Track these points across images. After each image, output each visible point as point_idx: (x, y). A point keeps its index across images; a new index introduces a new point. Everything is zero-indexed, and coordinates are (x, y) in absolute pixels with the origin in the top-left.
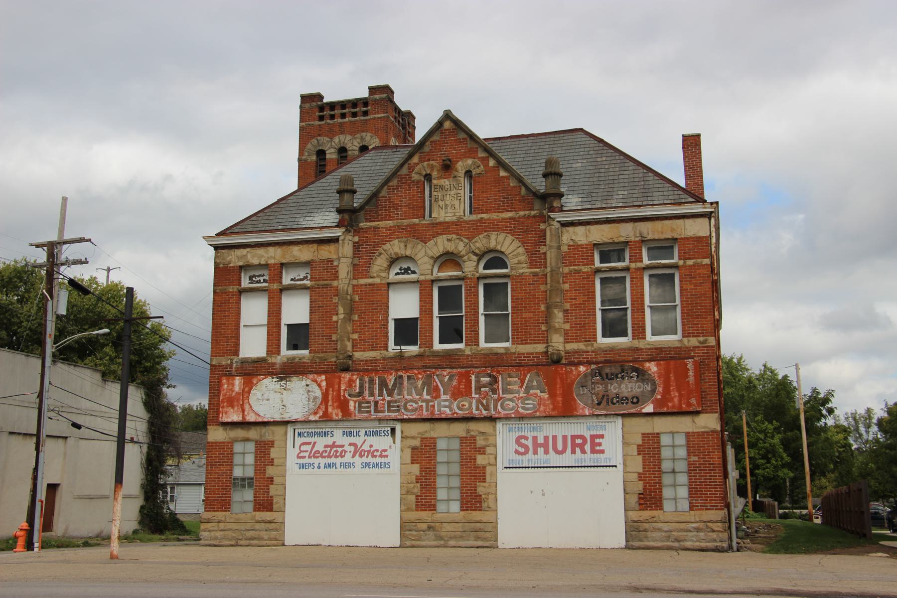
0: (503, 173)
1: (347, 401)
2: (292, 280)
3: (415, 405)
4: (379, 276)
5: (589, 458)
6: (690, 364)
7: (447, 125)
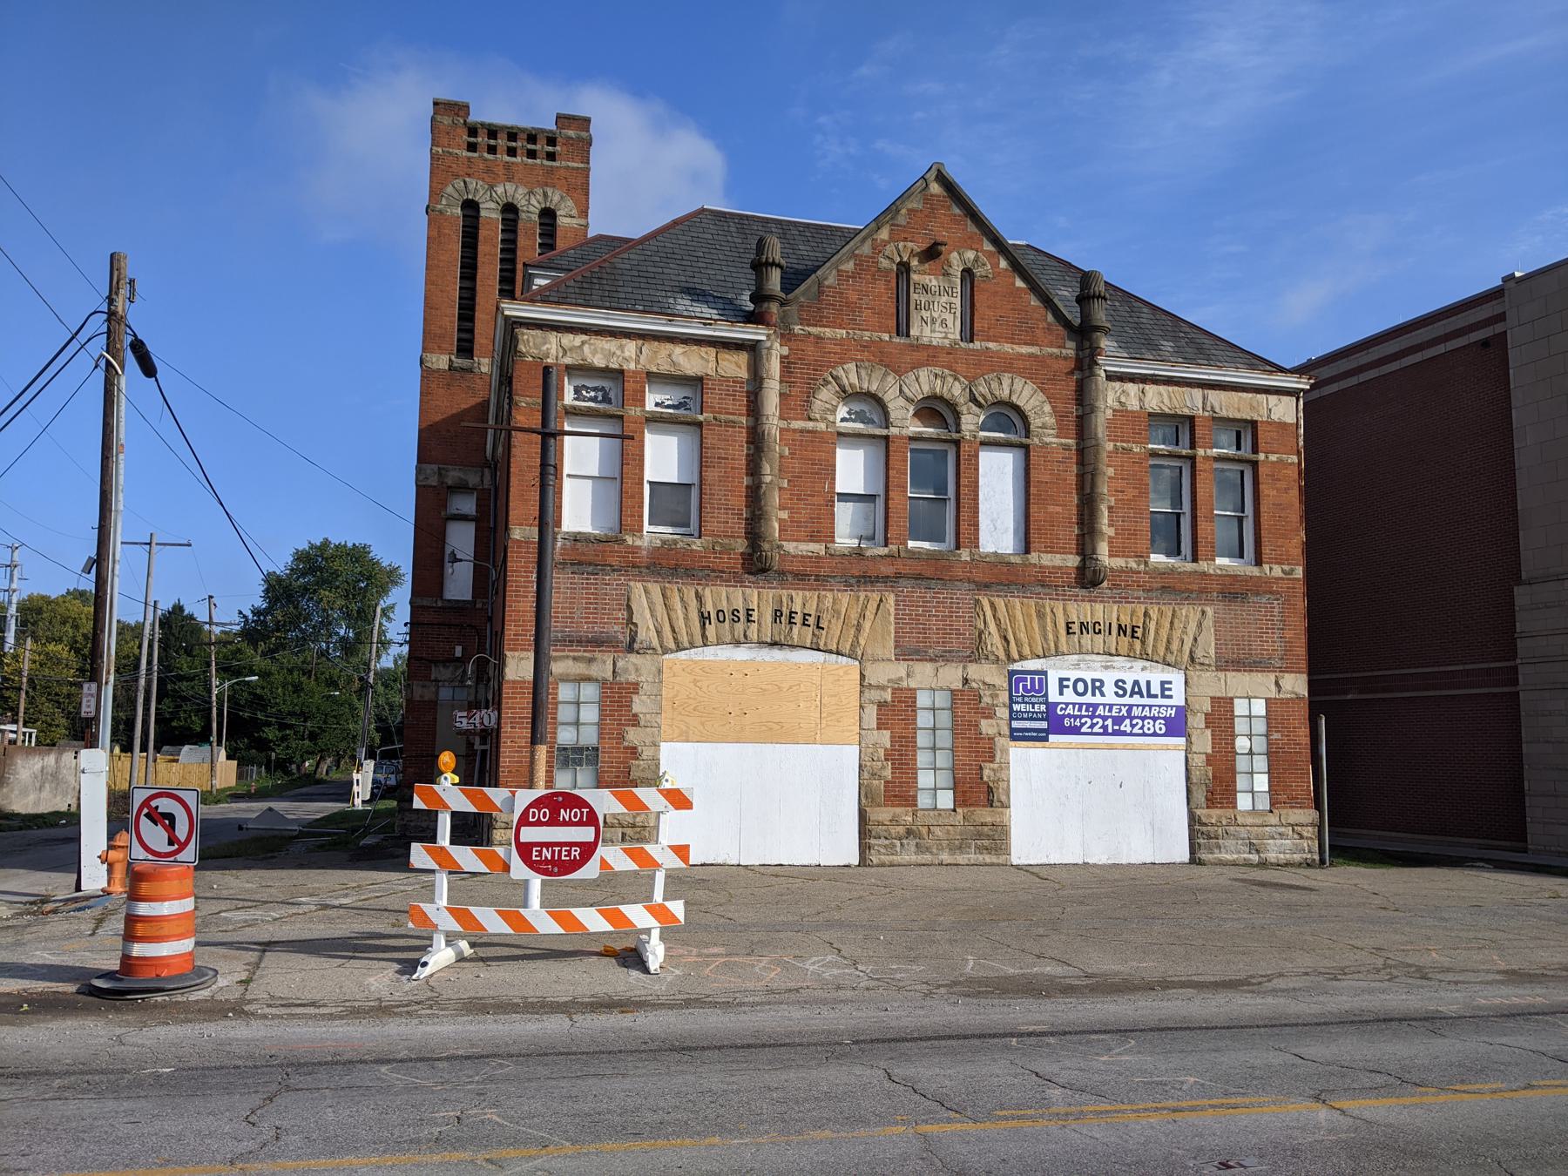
0: (1019, 283)
2: (657, 404)
4: (824, 419)
7: (935, 188)
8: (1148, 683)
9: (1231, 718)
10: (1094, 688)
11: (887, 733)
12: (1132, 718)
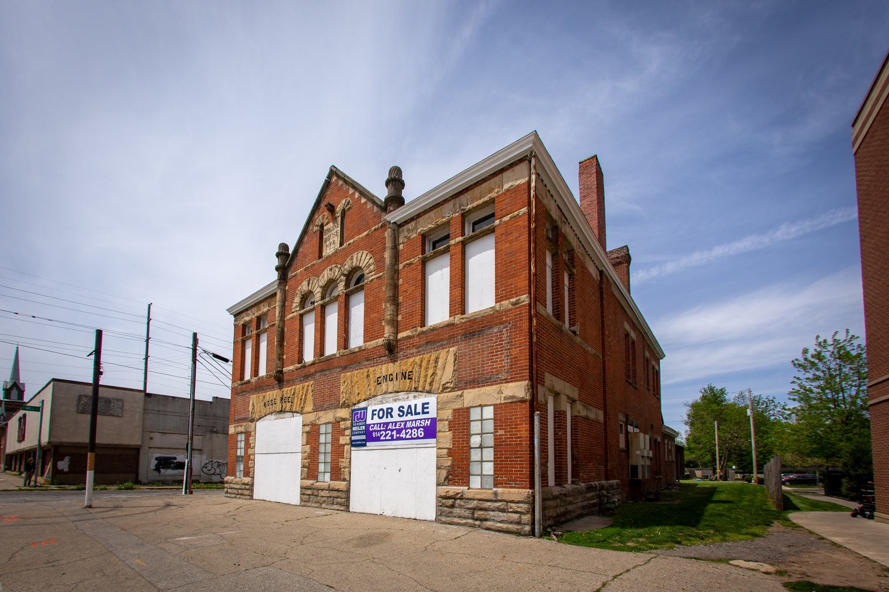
8: (416, 405)
9: (468, 423)
10: (388, 413)
12: (406, 429)
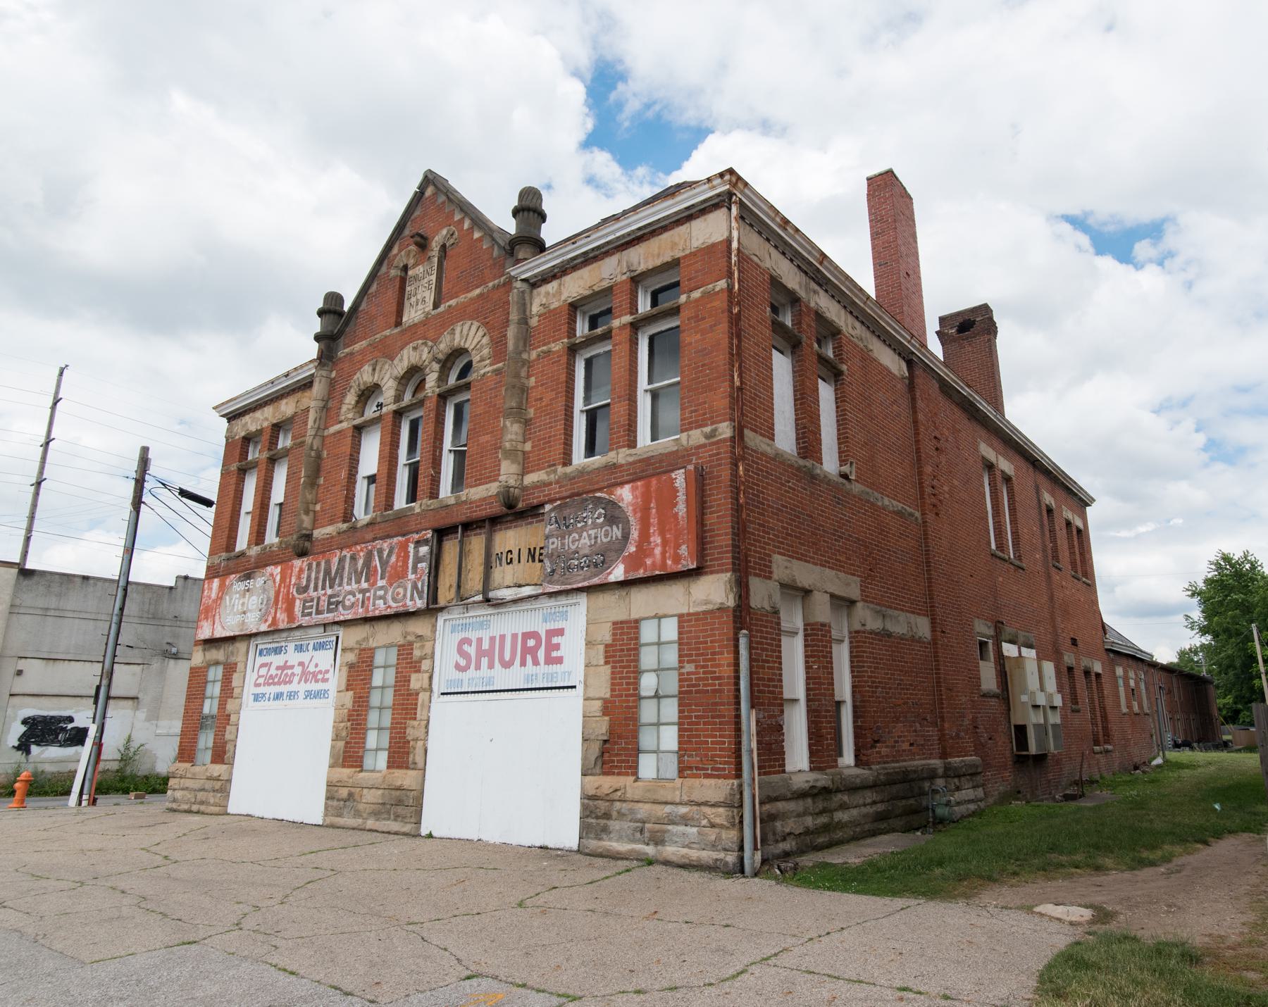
1: (294, 599)
3: (353, 599)
5: (541, 673)
6: (679, 478)
11: (351, 693)
